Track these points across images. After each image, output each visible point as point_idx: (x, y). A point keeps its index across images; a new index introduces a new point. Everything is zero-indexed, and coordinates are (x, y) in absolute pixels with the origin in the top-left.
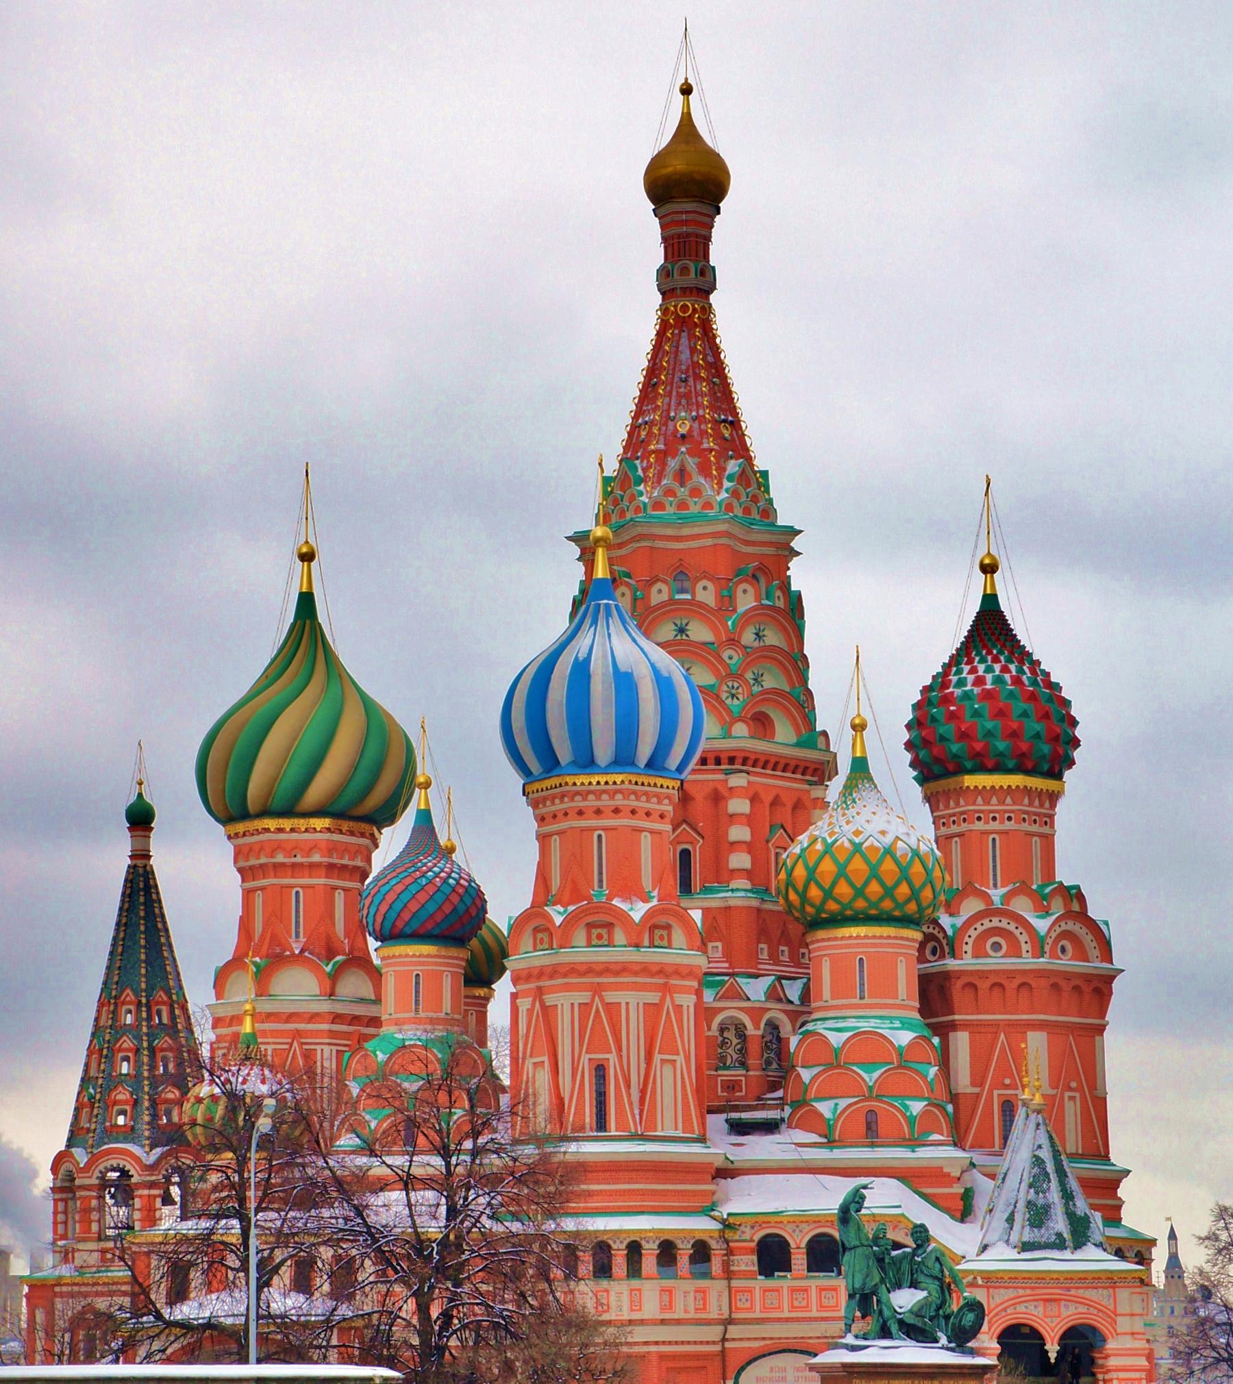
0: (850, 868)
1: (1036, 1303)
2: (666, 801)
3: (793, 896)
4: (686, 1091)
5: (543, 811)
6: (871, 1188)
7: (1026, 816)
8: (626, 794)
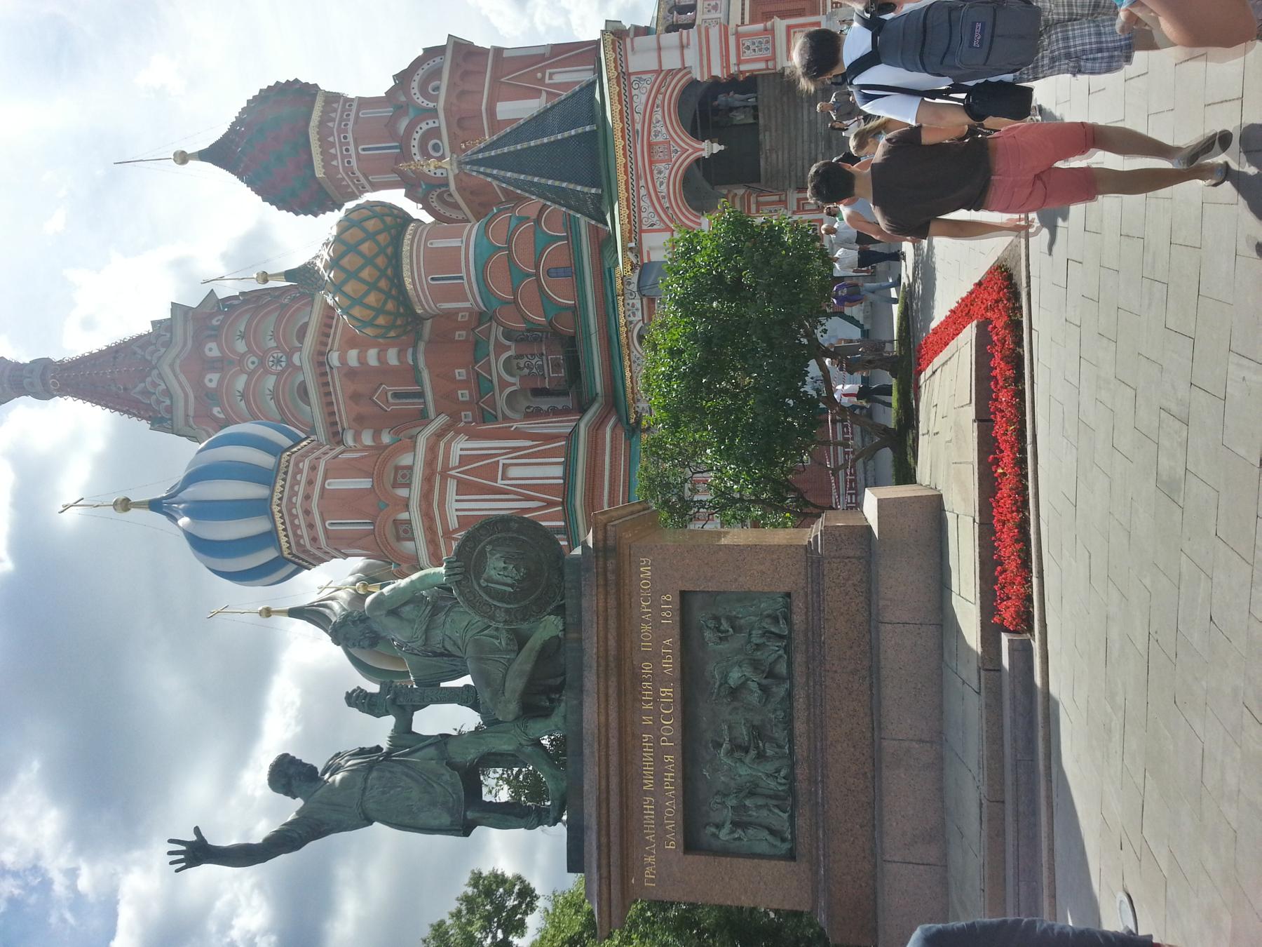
0: (351, 294)
1: (655, 172)
2: (301, 465)
3: (392, 334)
4: (528, 453)
5: (326, 558)
6: (197, 830)
7: (343, 123)
8: (291, 505)
